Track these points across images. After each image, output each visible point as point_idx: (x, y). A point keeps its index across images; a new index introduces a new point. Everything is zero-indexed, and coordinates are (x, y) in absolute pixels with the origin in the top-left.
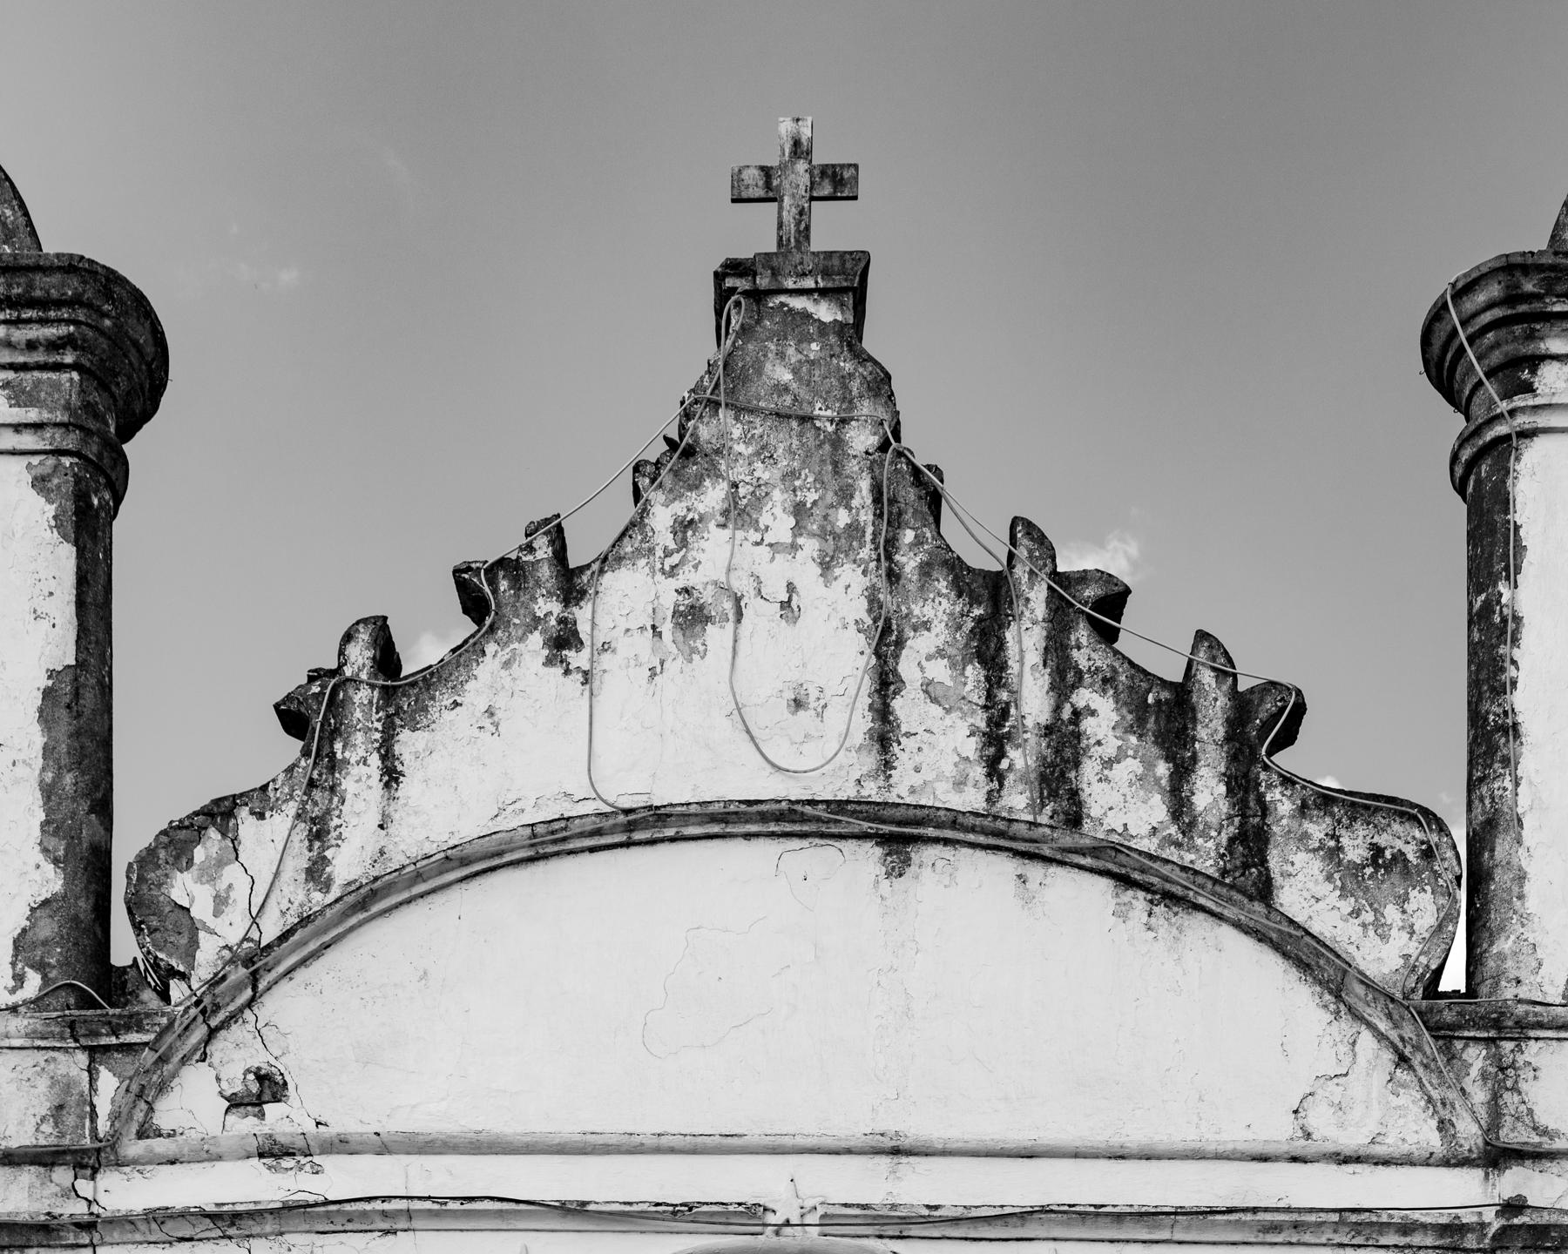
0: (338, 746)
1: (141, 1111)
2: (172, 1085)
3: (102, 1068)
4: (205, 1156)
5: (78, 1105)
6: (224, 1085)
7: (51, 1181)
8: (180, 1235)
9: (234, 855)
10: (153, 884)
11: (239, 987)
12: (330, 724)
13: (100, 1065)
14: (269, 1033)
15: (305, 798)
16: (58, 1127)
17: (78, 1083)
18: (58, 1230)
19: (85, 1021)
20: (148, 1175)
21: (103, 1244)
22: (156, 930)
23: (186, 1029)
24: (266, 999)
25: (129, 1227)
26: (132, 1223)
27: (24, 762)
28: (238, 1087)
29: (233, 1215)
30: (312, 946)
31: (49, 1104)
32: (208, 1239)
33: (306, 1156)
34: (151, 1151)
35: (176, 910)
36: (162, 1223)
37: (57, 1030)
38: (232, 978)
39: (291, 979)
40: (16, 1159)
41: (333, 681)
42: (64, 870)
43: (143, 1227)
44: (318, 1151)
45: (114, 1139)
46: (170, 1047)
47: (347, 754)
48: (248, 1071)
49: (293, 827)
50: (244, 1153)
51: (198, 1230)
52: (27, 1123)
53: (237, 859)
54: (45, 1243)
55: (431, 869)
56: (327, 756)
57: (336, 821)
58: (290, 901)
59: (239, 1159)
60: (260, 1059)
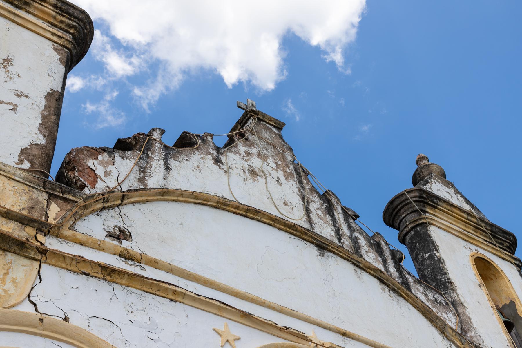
0: (150, 153)
1: (72, 221)
2: (84, 218)
3: (53, 202)
4: (98, 246)
5: (40, 210)
6: (106, 228)
7: (24, 231)
8: (84, 271)
9: (113, 164)
10: (81, 158)
11: (117, 198)
12: (147, 147)
13: (53, 201)
14: (125, 218)
15: (138, 161)
16: (29, 214)
17: (41, 203)
18: (28, 248)
19: (51, 184)
20: (70, 245)
21: (46, 262)
22: (80, 171)
23: (97, 201)
24: (124, 207)
25: (62, 259)
26: (64, 258)
27: (37, 105)
28: (111, 230)
29: (112, 270)
30: (144, 198)
31: (27, 205)
32: (96, 277)
33: (138, 263)
34: (75, 236)
35: (89, 169)
36: (79, 263)
37: (38, 182)
38: (116, 193)
39: (134, 205)
40: (10, 216)
41: (148, 138)
42: (47, 139)
43: (68, 261)
44: (144, 262)
45: (59, 226)
46: (90, 204)
47: (153, 156)
48: (115, 226)
49: (135, 166)
50: (114, 252)
51: (93, 271)
52: (15, 207)
53: (114, 165)
54: (18, 252)
55: (186, 194)
56: (146, 154)
57: (148, 171)
58: (132, 184)
59: (111, 253)
60: (121, 224)
